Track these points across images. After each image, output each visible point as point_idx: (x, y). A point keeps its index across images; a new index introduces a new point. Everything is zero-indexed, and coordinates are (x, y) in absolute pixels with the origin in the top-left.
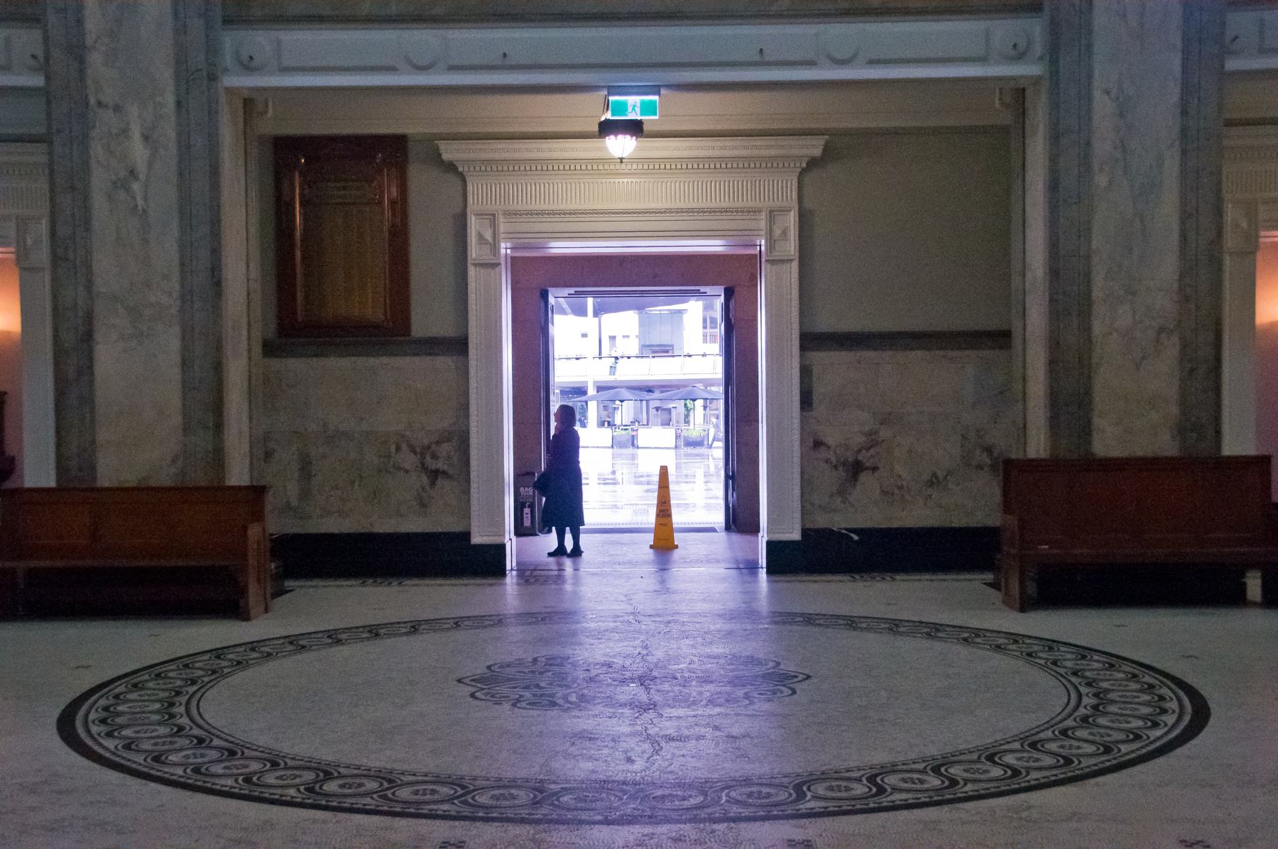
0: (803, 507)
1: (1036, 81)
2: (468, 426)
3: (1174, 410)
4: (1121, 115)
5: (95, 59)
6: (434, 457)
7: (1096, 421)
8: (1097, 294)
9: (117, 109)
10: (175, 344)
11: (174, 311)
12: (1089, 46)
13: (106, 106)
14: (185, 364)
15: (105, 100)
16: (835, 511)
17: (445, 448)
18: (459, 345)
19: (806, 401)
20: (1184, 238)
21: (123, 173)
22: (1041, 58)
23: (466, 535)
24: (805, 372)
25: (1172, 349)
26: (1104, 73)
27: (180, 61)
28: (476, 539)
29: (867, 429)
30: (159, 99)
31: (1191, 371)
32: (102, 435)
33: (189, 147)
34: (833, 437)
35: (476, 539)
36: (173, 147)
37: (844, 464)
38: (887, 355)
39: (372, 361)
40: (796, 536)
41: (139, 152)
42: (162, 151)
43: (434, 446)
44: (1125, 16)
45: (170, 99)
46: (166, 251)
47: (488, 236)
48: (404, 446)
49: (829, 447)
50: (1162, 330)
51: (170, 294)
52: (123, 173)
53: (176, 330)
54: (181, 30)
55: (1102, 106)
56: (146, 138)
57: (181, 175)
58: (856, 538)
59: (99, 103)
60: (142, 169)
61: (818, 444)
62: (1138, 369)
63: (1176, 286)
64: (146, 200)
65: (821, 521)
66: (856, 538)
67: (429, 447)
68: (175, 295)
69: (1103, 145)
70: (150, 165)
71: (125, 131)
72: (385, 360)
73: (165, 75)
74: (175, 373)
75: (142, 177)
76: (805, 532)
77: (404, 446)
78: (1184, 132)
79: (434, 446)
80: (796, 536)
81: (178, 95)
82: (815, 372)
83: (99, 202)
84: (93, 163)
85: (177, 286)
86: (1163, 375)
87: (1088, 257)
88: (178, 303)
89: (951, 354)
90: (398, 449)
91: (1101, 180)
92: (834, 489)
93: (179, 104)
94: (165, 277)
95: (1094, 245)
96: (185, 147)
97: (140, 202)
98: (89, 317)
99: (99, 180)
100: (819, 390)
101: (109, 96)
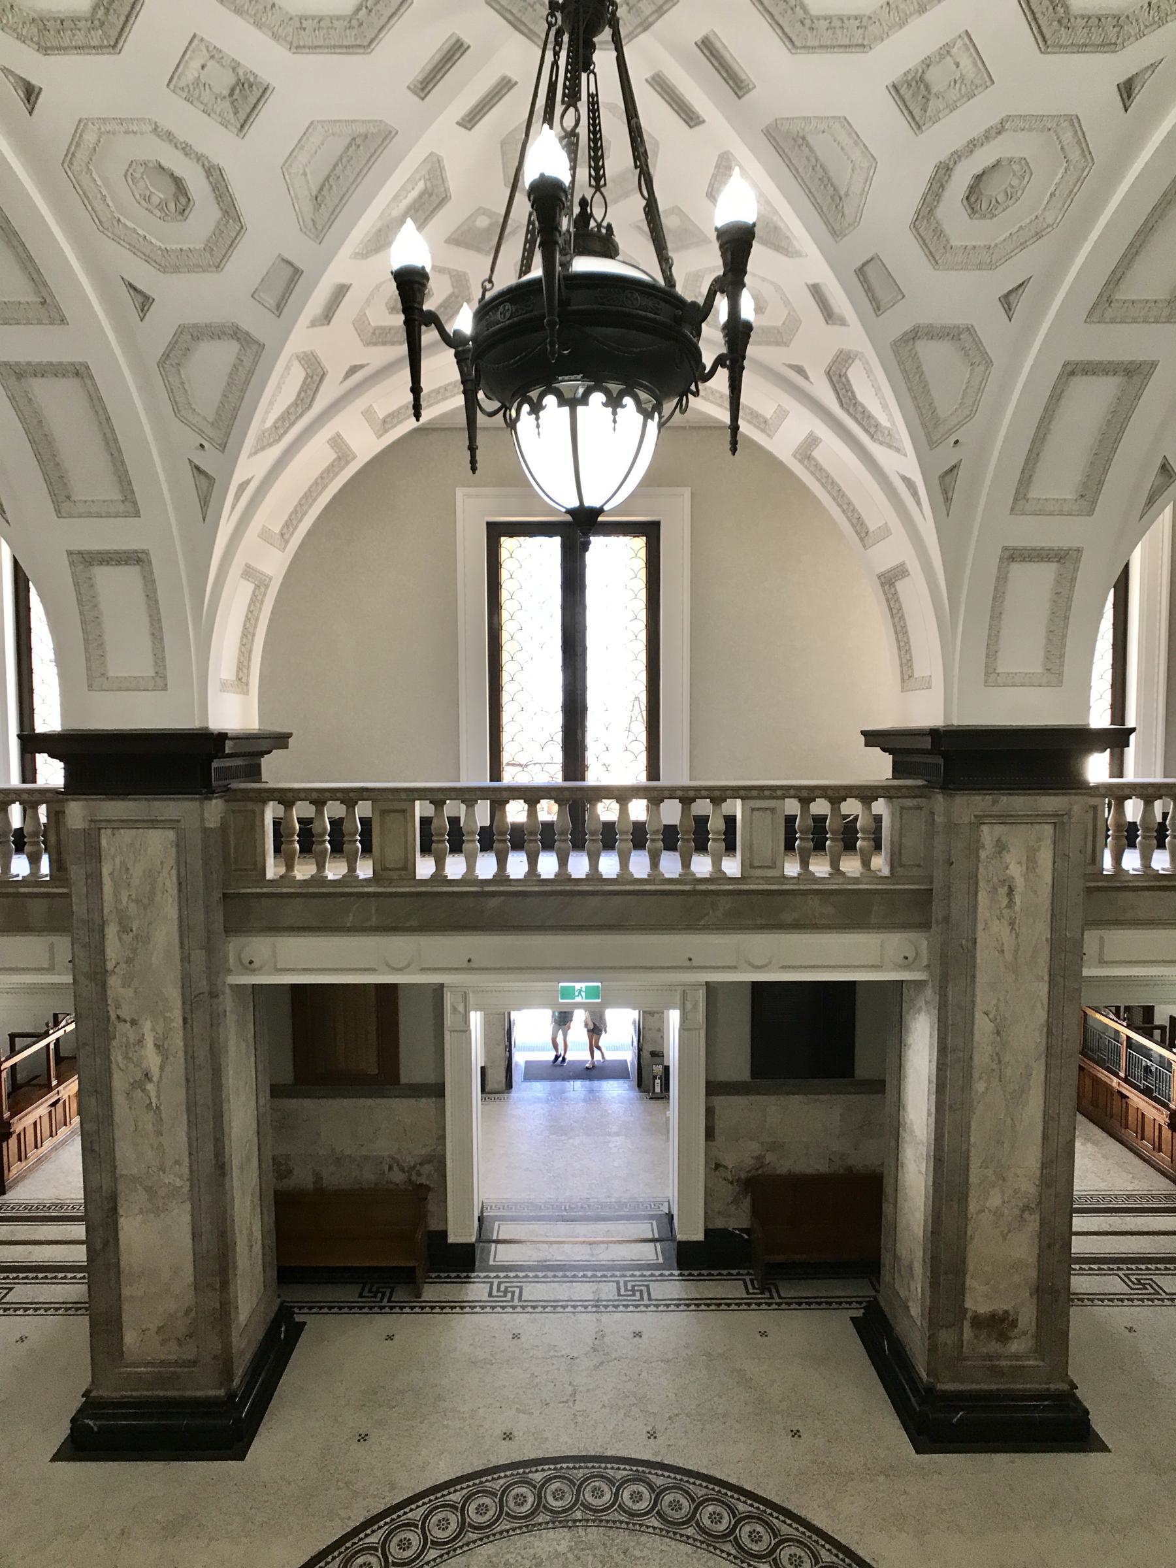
0: (706, 1213)
1: (919, 985)
2: (444, 1150)
3: (1034, 1273)
4: (998, 1033)
5: (113, 982)
6: (419, 1174)
7: (969, 1282)
8: (973, 1180)
9: (134, 1022)
10: (187, 1218)
11: (186, 1190)
12: (974, 976)
13: (125, 1021)
14: (195, 1236)
15: (123, 1016)
16: (730, 1216)
17: (427, 1168)
18: (437, 1091)
19: (710, 1134)
20: (1045, 1137)
21: (139, 1076)
22: (928, 966)
23: (444, 1234)
24: (710, 1112)
25: (1033, 1223)
26: (984, 1000)
27: (186, 981)
28: (451, 1239)
29: (756, 1154)
30: (168, 1014)
31: (1049, 1246)
32: (126, 1292)
33: (193, 1057)
34: (730, 1160)
35: (451, 1239)
36: (181, 1054)
37: (739, 1180)
38: (773, 1098)
39: (369, 1102)
40: (700, 1237)
41: (152, 1060)
42: (171, 1058)
43: (418, 1167)
44: (1003, 951)
45: (177, 1015)
46: (178, 1138)
47: (461, 1008)
48: (395, 1168)
49: (726, 1168)
50: (1026, 1208)
51: (181, 1177)
52: (139, 1076)
53: (188, 1206)
54: (186, 959)
55: (983, 1026)
56: (157, 1046)
57: (188, 1080)
58: (746, 1237)
59: (118, 1017)
60: (155, 1072)
61: (718, 1166)
62: (1005, 1239)
63: (1038, 1173)
64: (158, 1097)
65: (720, 1223)
66: (746, 1237)
67: (415, 1167)
68: (186, 1177)
69: (982, 1057)
70: (162, 1069)
71: (140, 1041)
72: (378, 1101)
73: (173, 994)
74: (188, 1241)
75: (155, 1079)
76: (707, 1232)
77: (395, 1168)
78: (1048, 1048)
79: (418, 1167)
80: (700, 1237)
81: (184, 1013)
82: (717, 1113)
83: (119, 1099)
84: (114, 1066)
85: (187, 1170)
86: (1023, 1247)
87: (968, 1151)
88: (188, 1183)
89: (822, 1097)
90: (390, 1168)
91: (980, 1086)
92: (730, 1199)
93: (185, 1020)
94: (177, 1162)
95: (972, 1140)
96: (190, 1056)
97: (154, 1100)
98: (113, 1198)
99: (119, 1082)
100: (720, 1125)
101: (125, 1013)
